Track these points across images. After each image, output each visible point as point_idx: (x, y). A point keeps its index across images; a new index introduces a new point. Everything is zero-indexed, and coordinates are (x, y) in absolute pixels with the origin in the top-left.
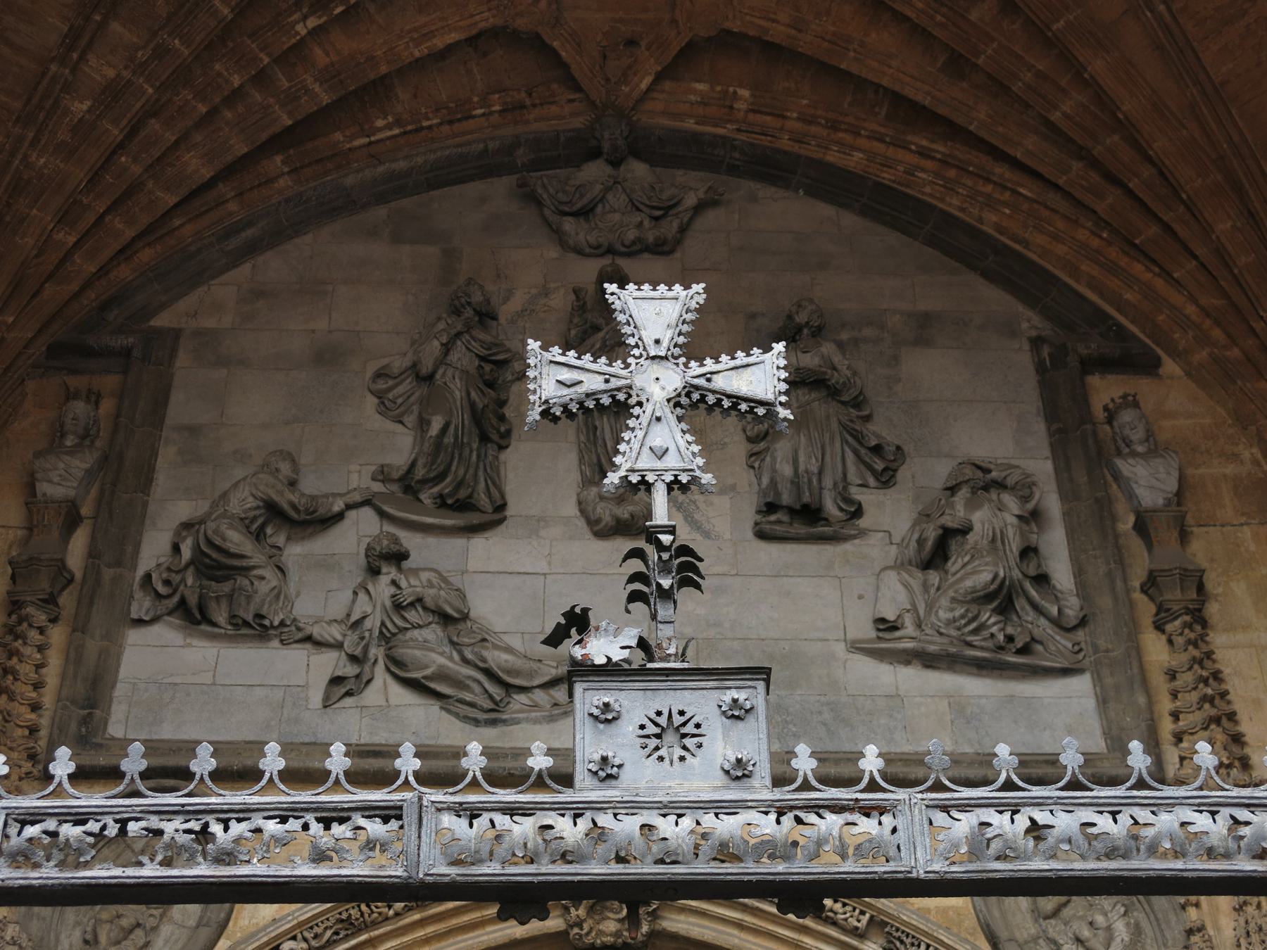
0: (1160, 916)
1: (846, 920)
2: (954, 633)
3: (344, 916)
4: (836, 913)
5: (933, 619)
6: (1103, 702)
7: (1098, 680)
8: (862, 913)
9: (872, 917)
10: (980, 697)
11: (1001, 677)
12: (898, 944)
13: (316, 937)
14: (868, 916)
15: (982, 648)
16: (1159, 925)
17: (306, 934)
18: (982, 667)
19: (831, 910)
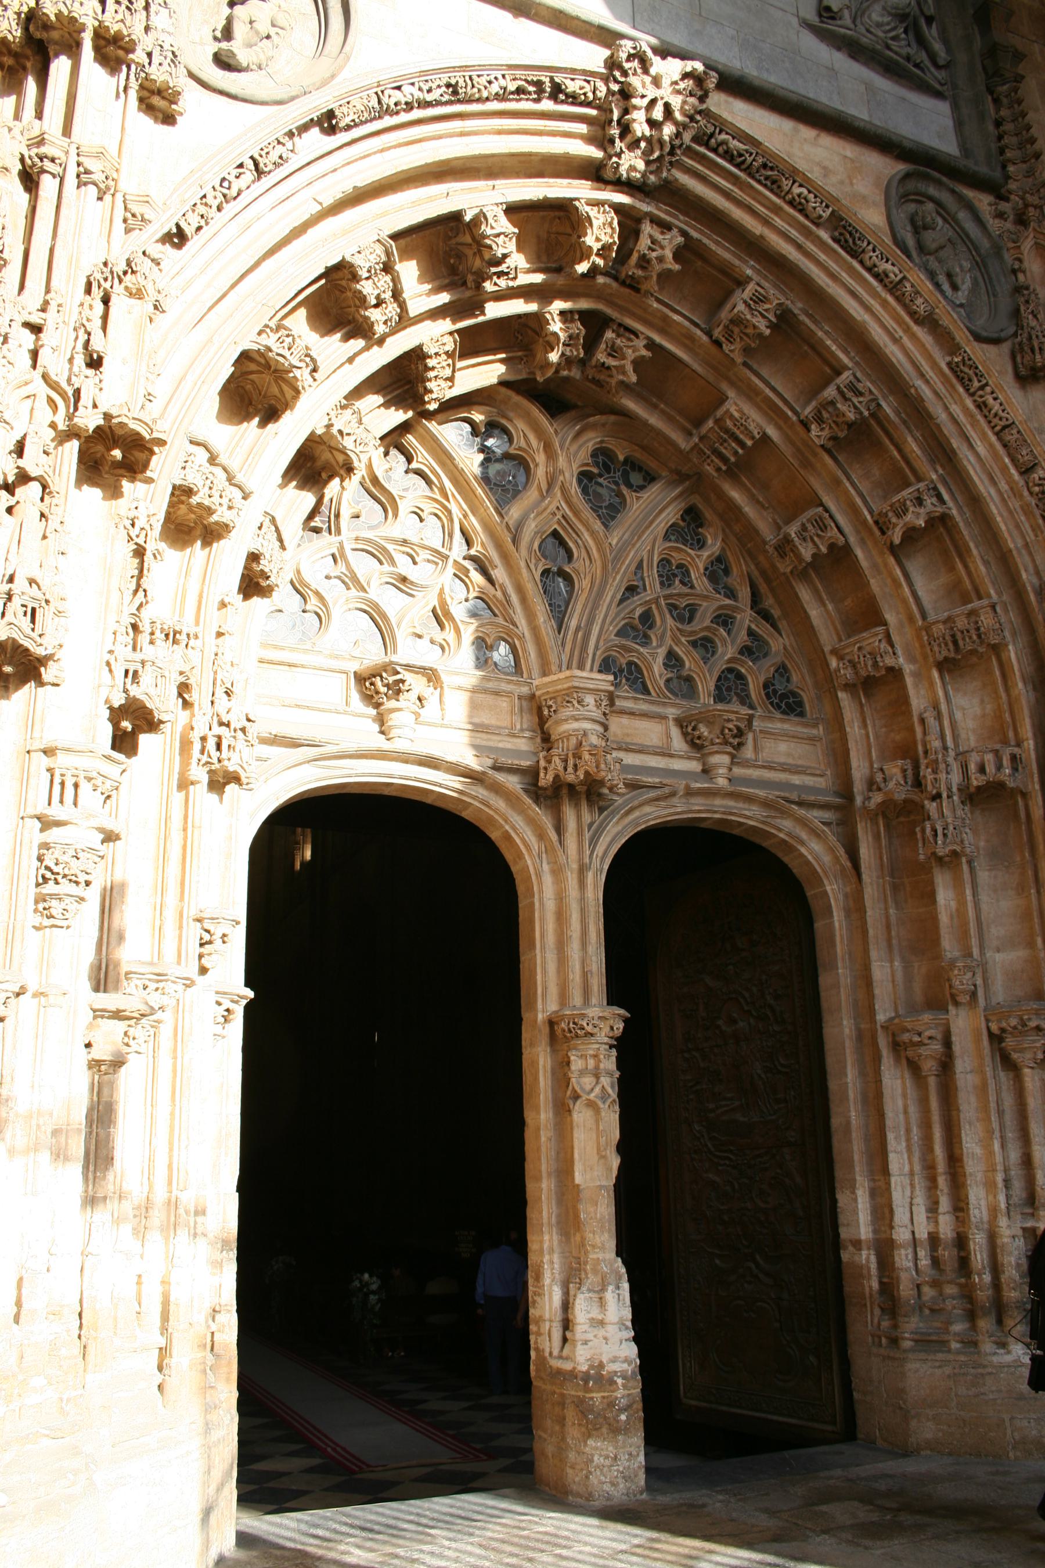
0: (993, 276)
1: (815, 208)
2: (881, 34)
3: (453, 82)
4: (807, 201)
5: (866, 19)
6: (959, 125)
7: (955, 107)
8: (827, 206)
9: (833, 212)
10: (885, 91)
11: (897, 82)
12: (848, 236)
13: (429, 91)
14: (831, 209)
15: (896, 53)
16: (990, 279)
17: (421, 84)
18: (891, 69)
19: (805, 199)
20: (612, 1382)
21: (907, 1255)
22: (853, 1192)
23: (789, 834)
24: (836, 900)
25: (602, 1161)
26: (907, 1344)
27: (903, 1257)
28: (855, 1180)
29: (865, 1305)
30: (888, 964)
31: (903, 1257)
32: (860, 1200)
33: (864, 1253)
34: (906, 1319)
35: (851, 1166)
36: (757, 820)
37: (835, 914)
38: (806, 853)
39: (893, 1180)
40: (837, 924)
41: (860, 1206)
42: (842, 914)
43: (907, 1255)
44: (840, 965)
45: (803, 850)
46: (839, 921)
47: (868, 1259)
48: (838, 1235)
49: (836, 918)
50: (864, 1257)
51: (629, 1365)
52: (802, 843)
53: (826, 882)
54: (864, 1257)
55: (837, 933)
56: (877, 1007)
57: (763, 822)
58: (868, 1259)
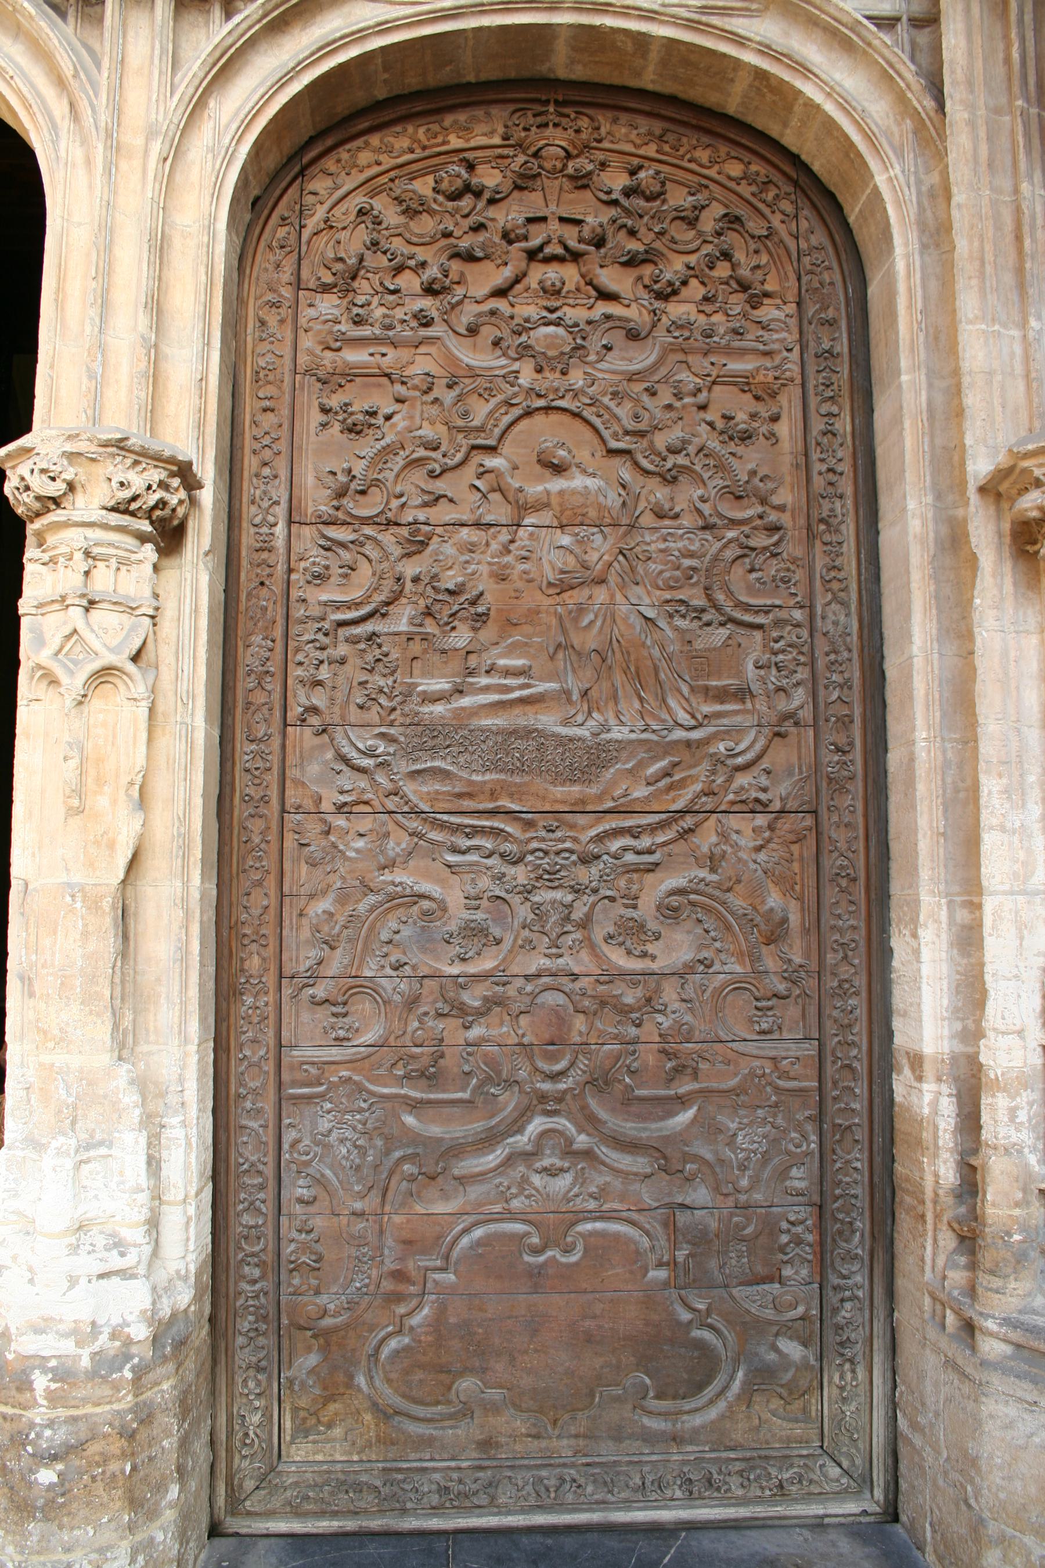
20: (25, 1385)
21: (1013, 1112)
22: (915, 935)
23: (766, 50)
24: (898, 204)
25: (76, 822)
26: (992, 1348)
27: (1003, 1116)
28: (917, 902)
29: (923, 1216)
30: (1016, 333)
31: (1003, 1116)
32: (926, 954)
33: (929, 1088)
34: (996, 1283)
35: (913, 871)
36: (676, 21)
37: (897, 240)
38: (818, 97)
39: (989, 905)
40: (900, 265)
41: (926, 969)
42: (913, 236)
43: (1013, 1112)
44: (904, 363)
45: (810, 90)
46: (907, 256)
47: (935, 1104)
48: (890, 1034)
49: (899, 250)
50: (927, 1098)
51: (79, 1344)
52: (804, 70)
53: (873, 164)
54: (927, 1098)
55: (902, 287)
56: (969, 441)
57: (691, 25)
58: (935, 1104)
